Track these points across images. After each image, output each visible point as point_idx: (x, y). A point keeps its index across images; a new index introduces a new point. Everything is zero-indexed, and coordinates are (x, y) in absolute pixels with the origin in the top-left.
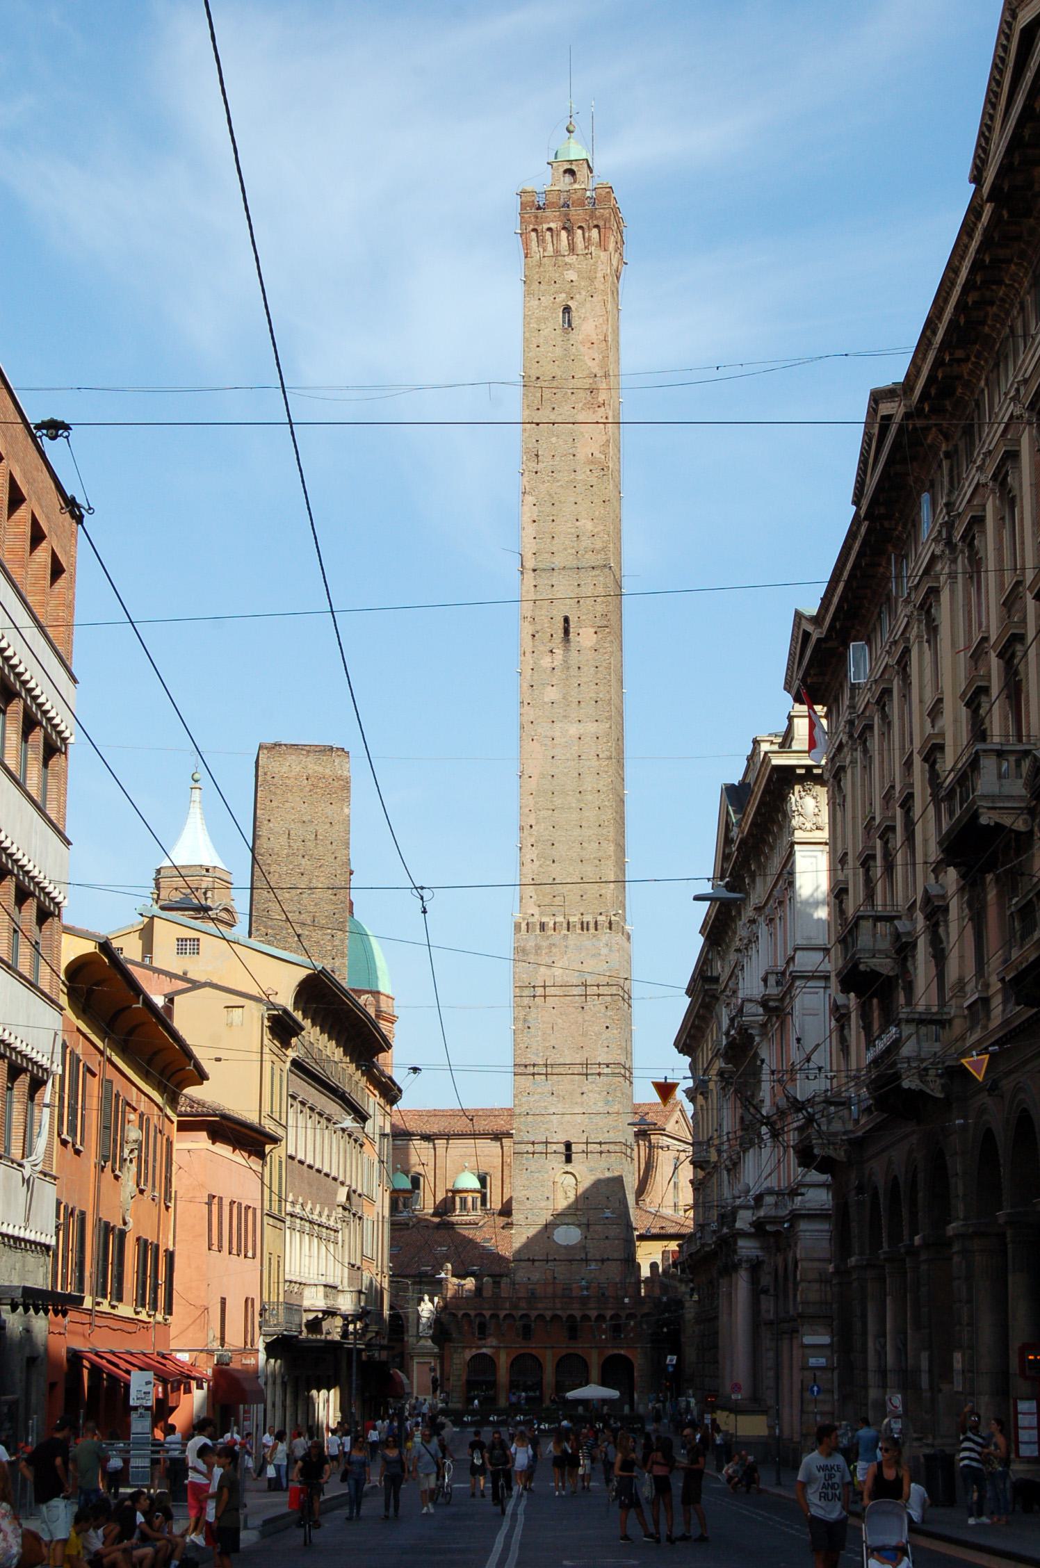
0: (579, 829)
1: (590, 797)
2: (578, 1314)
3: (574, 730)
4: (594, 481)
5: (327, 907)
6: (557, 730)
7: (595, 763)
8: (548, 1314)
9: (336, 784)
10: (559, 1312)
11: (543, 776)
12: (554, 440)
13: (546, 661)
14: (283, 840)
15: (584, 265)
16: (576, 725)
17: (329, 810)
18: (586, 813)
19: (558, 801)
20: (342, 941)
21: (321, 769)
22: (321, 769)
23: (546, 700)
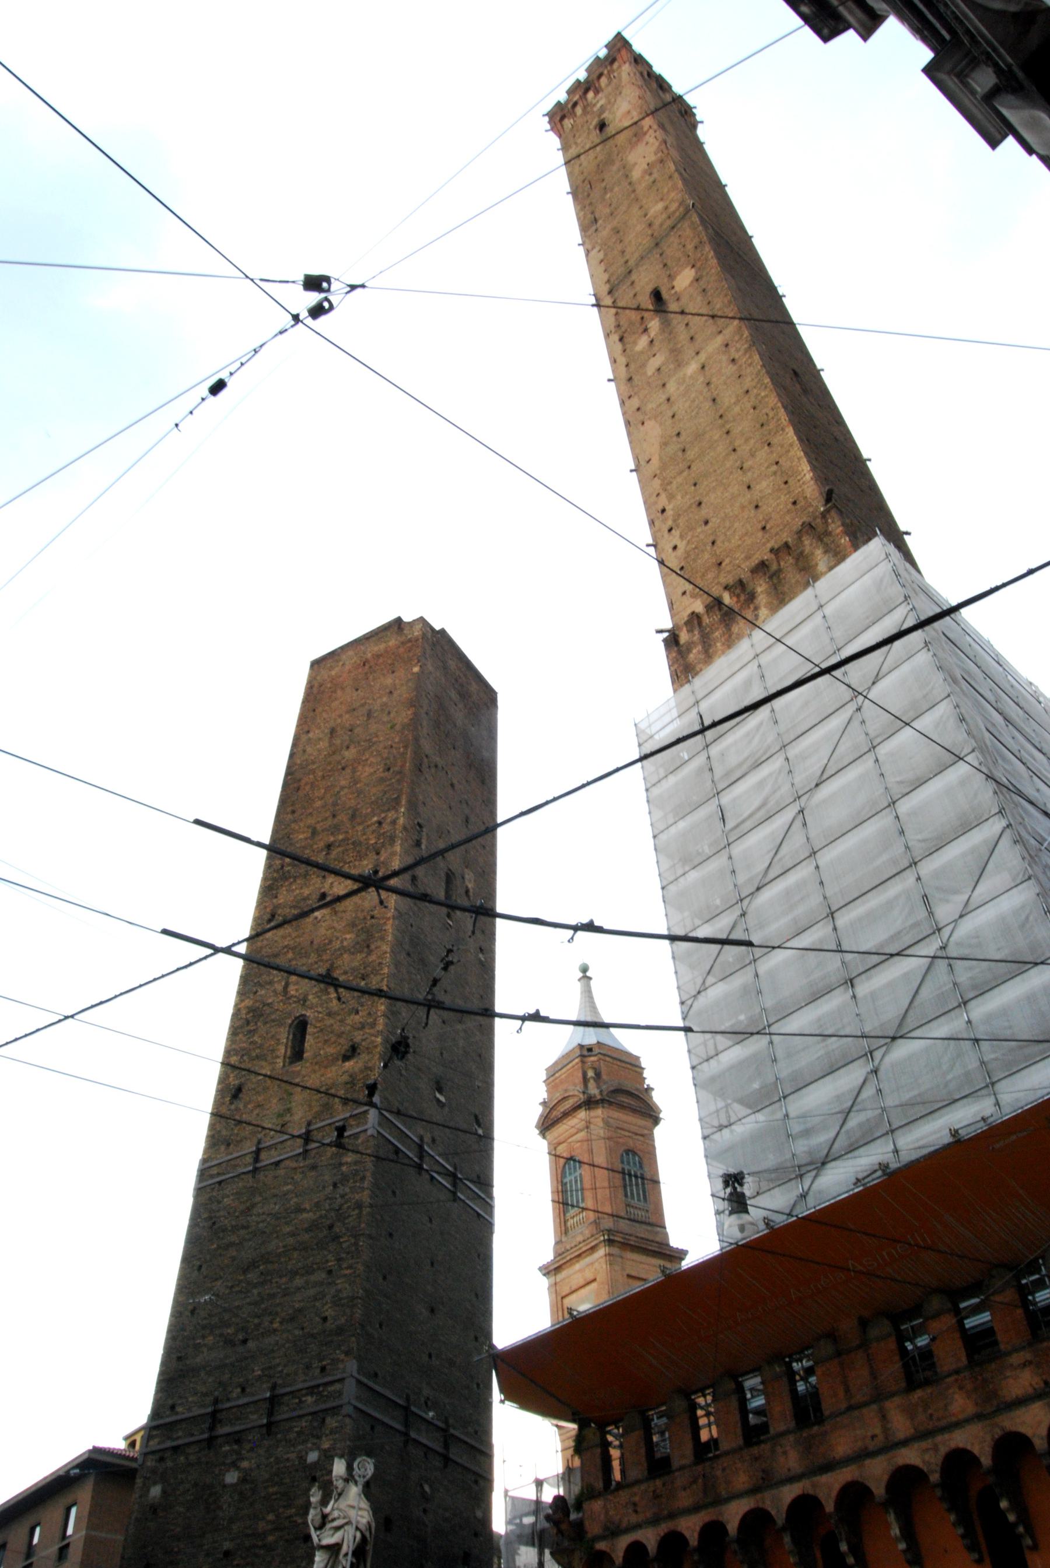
0: (733, 456)
1: (737, 409)
2: (976, 1440)
3: (692, 368)
4: (655, 175)
5: (374, 790)
6: (672, 387)
7: (732, 369)
8: (876, 1473)
9: (401, 650)
10: (910, 1456)
11: (665, 444)
12: (608, 196)
13: (643, 342)
14: (323, 745)
15: (610, 89)
16: (696, 358)
17: (389, 681)
18: (736, 431)
19: (691, 454)
20: (394, 822)
21: (382, 646)
22: (382, 646)
23: (650, 373)
